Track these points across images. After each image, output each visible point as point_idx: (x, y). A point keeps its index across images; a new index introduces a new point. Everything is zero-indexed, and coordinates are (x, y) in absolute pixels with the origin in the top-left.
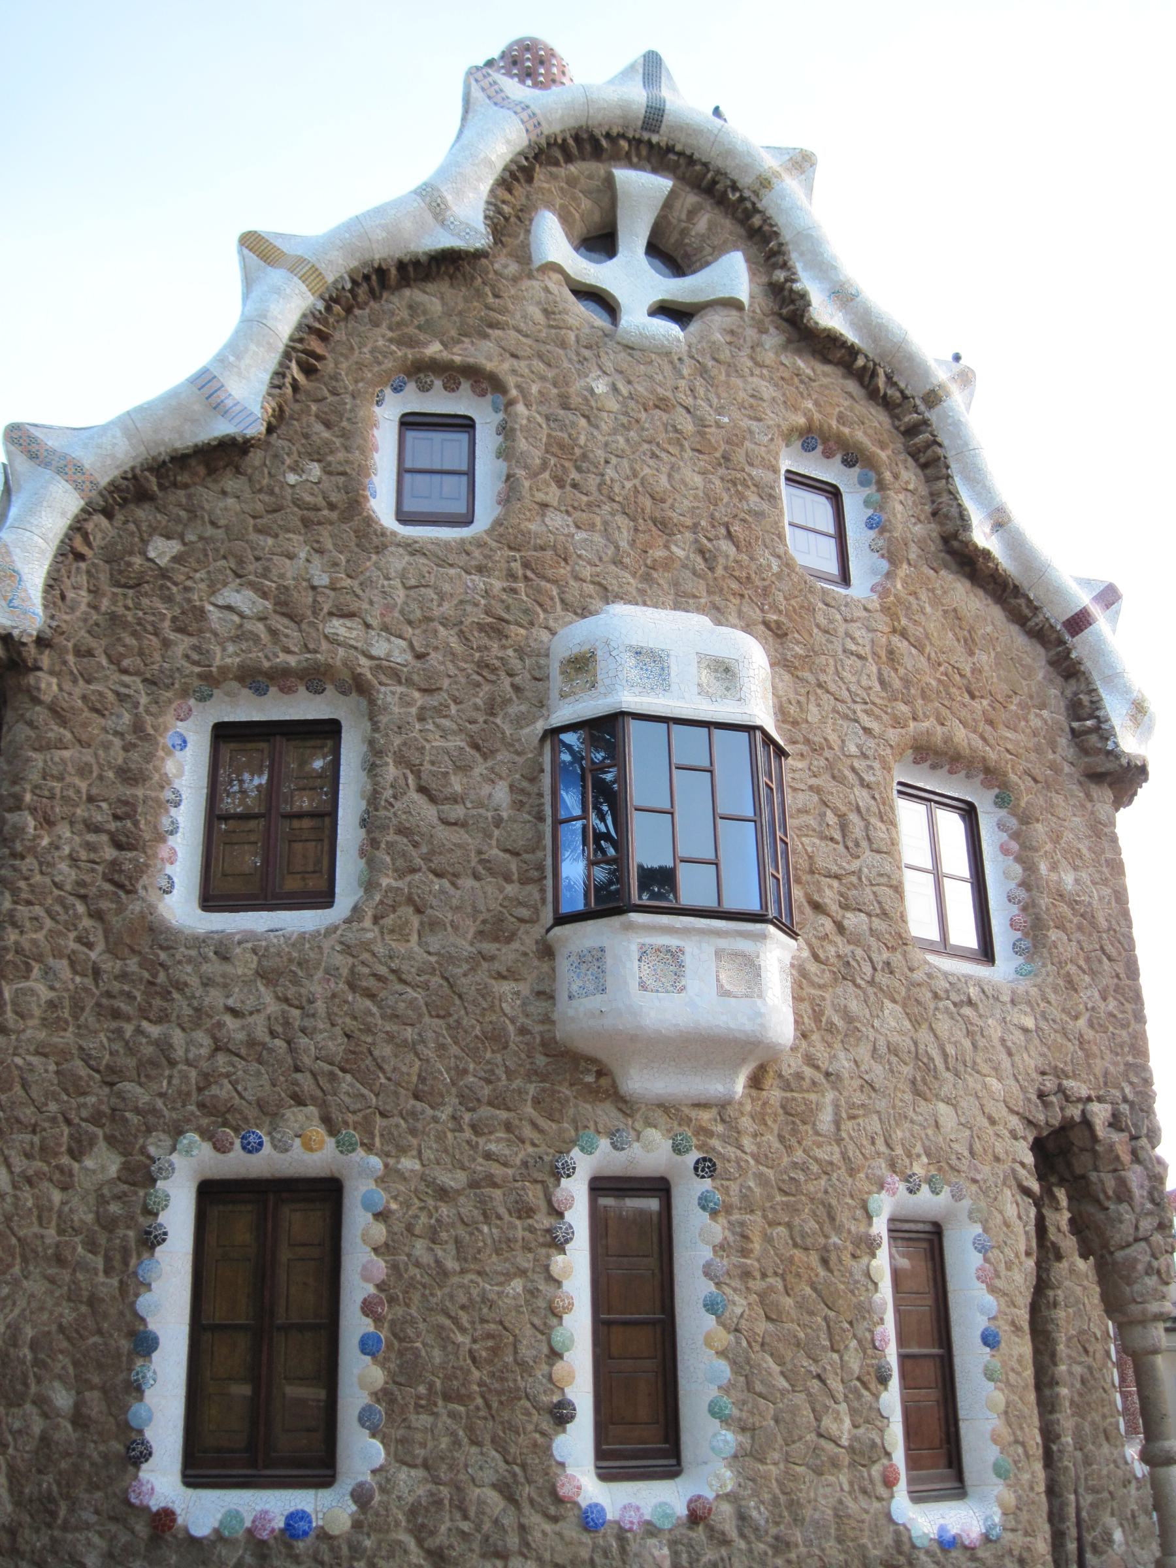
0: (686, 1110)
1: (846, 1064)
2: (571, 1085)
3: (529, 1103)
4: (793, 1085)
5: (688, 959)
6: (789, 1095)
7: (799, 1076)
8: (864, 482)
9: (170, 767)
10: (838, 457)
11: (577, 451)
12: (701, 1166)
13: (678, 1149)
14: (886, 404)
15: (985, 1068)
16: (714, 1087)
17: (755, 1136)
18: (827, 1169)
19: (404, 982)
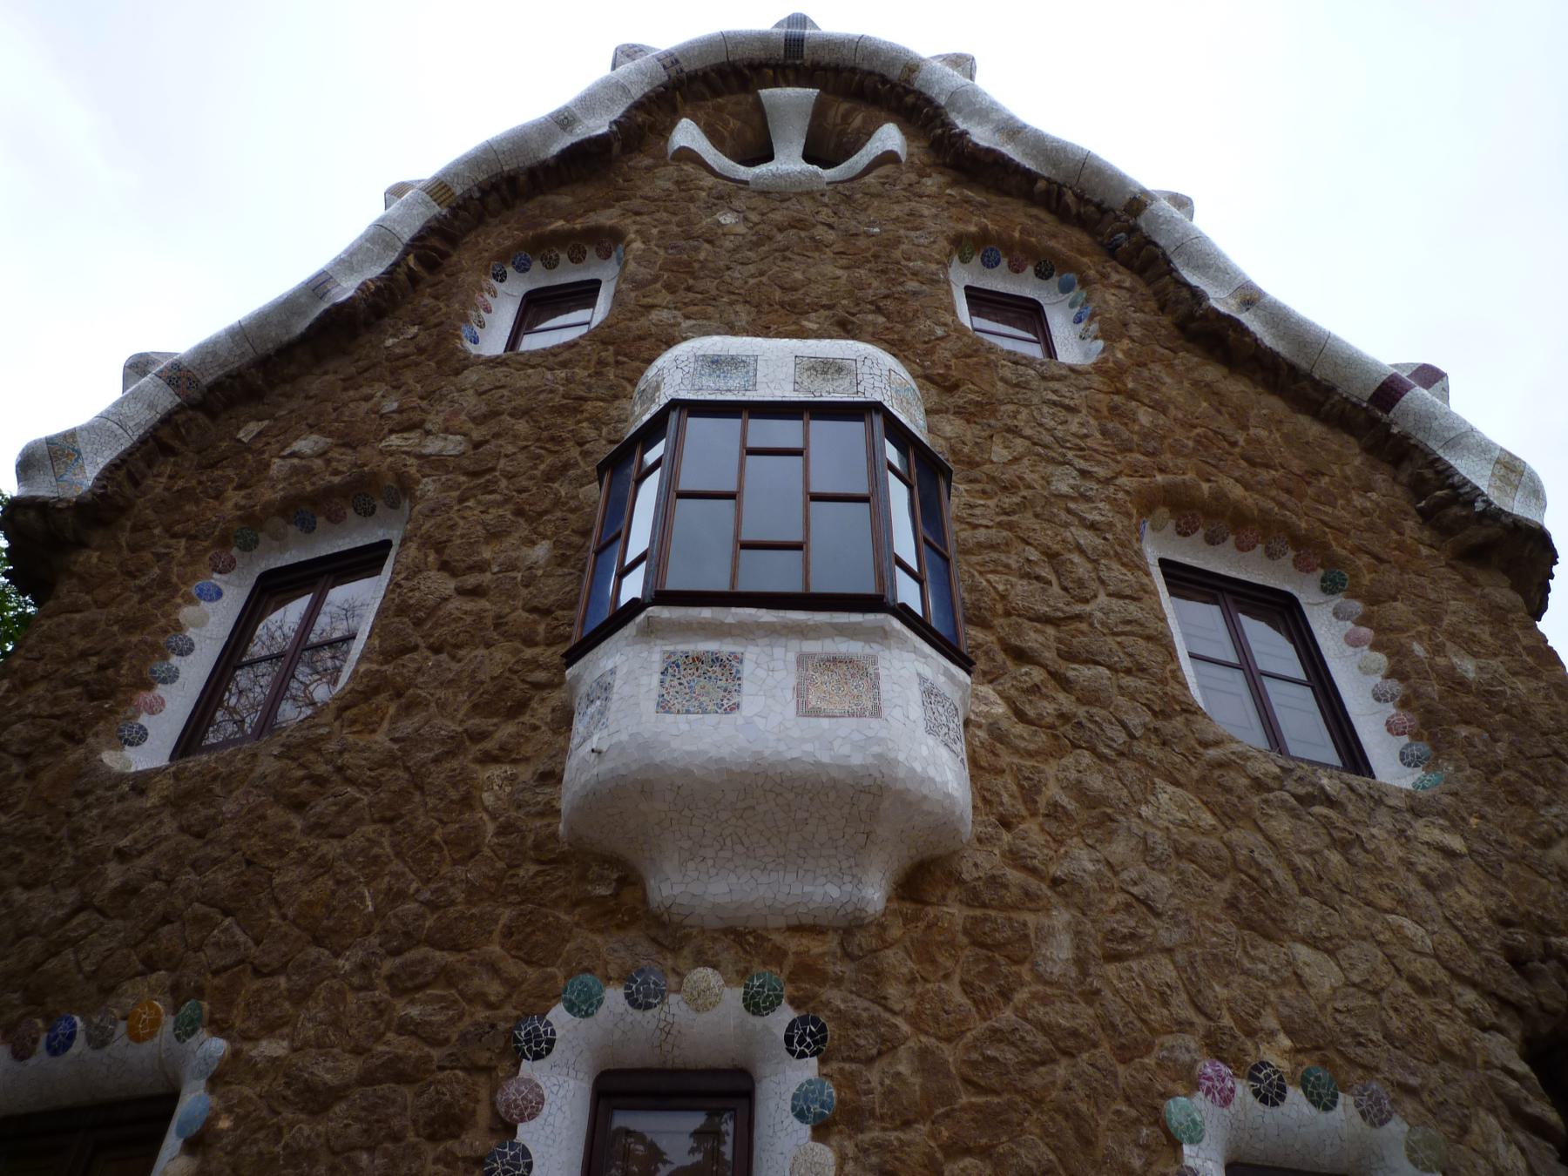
0: (777, 938)
1: (1090, 867)
2: (576, 904)
3: (496, 936)
4: (986, 897)
5: (747, 669)
6: (978, 912)
7: (994, 881)
8: (1065, 288)
9: (186, 613)
10: (1030, 269)
11: (696, 265)
12: (797, 1033)
13: (756, 1004)
14: (1082, 222)
15: (1385, 901)
16: (822, 891)
17: (912, 981)
18: (1068, 1044)
19: (350, 781)
